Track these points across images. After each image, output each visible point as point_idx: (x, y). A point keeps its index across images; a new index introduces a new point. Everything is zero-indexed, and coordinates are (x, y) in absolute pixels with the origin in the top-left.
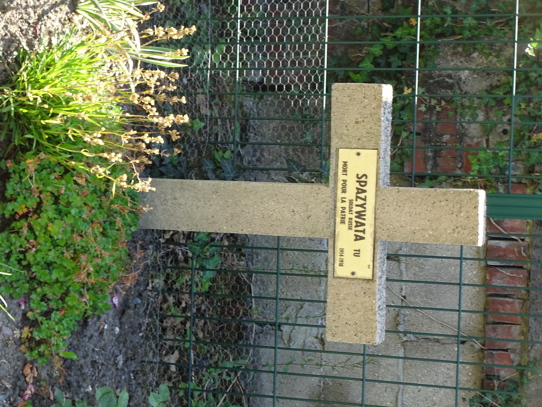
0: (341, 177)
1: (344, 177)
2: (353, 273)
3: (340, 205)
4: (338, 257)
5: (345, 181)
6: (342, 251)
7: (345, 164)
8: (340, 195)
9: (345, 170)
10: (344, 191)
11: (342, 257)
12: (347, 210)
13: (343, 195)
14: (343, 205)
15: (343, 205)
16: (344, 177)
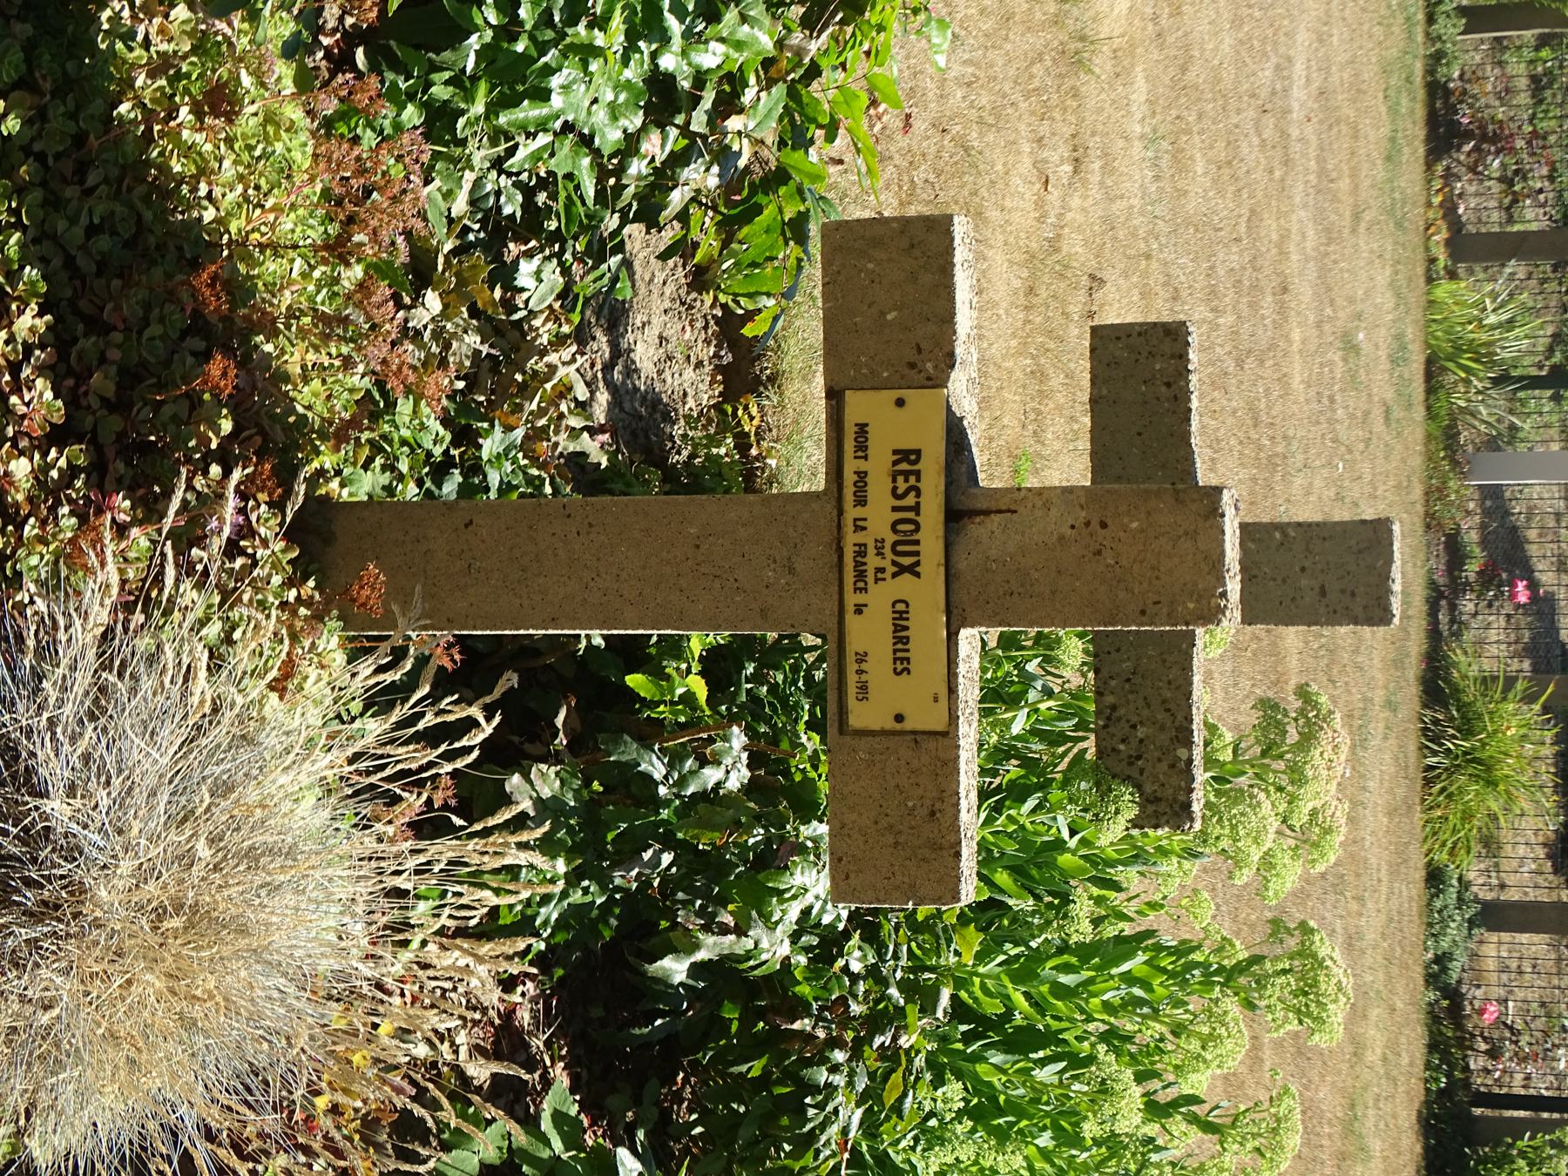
0: (851, 466)
1: (862, 465)
2: (899, 718)
3: (851, 539)
4: (852, 679)
5: (862, 476)
6: (861, 658)
7: (862, 429)
8: (851, 512)
9: (862, 447)
10: (861, 501)
11: (864, 677)
12: (871, 551)
13: (859, 512)
14: (860, 538)
15: (860, 538)
16: (862, 465)
